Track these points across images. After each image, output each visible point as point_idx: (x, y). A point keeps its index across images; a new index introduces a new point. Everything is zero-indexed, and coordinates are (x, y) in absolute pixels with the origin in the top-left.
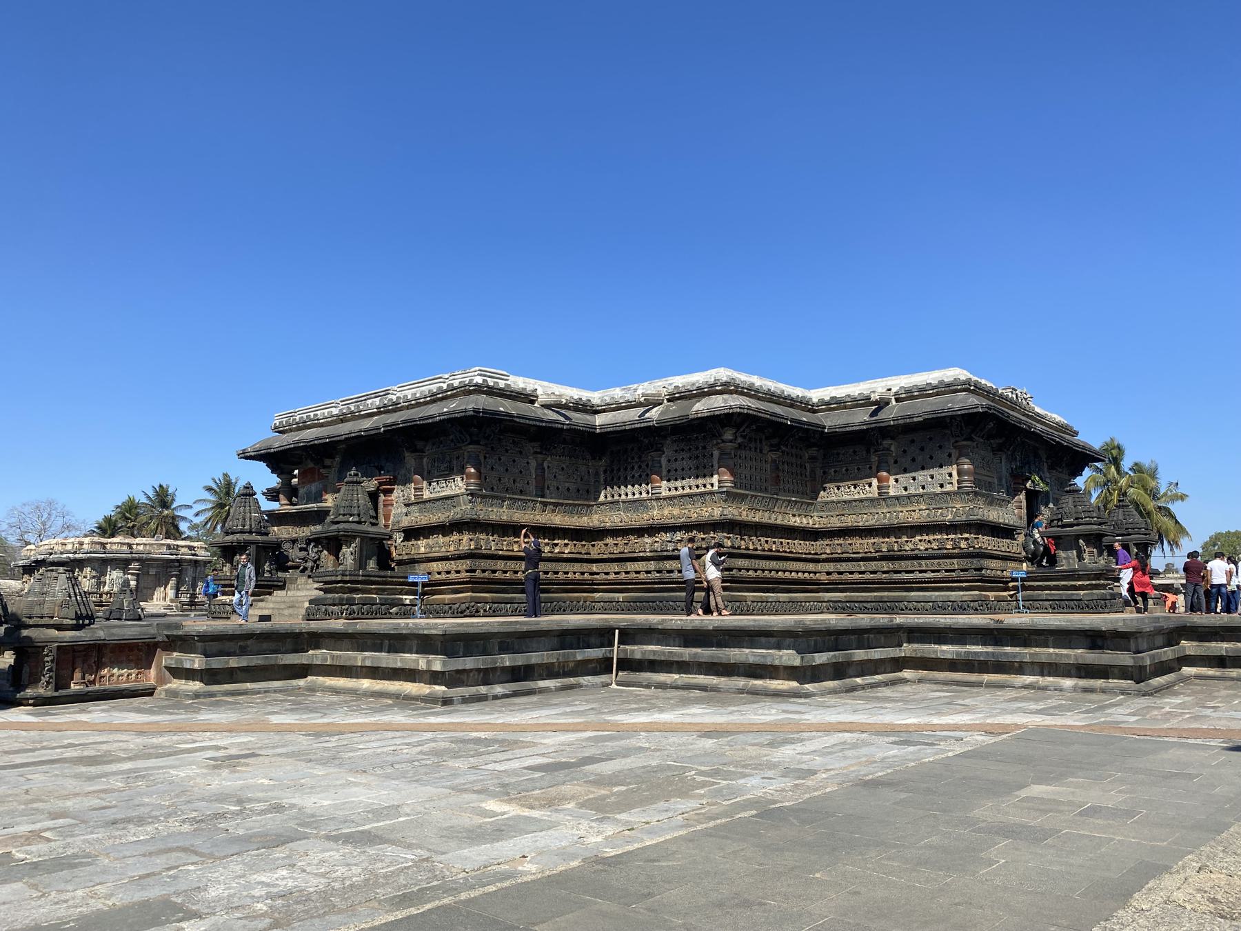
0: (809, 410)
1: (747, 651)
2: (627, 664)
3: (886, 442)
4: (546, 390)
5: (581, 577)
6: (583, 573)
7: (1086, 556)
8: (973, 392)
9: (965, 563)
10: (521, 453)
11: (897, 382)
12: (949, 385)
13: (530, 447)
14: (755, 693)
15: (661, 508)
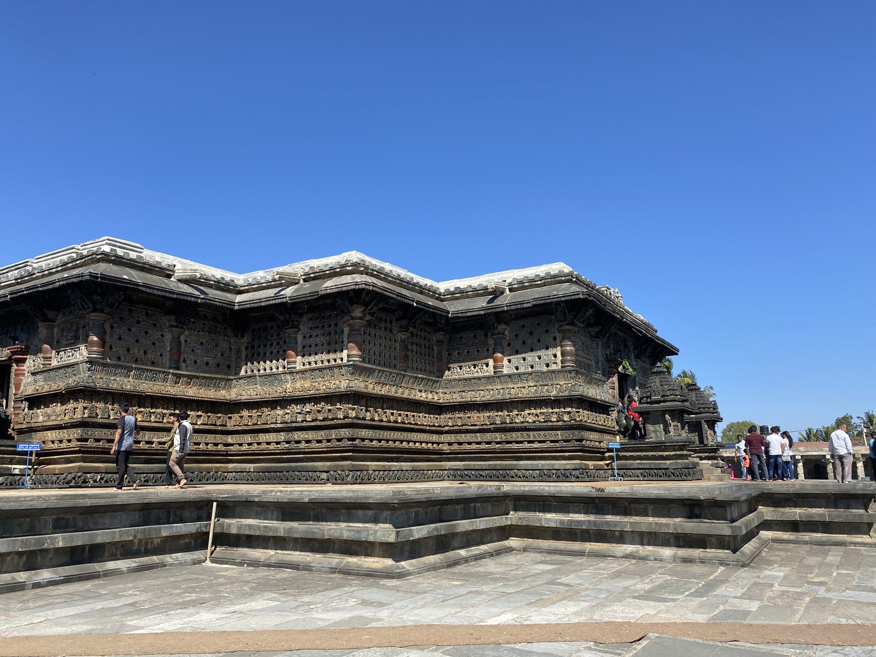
0: (437, 299)
1: (343, 525)
2: (223, 539)
3: (501, 327)
4: (183, 266)
5: (214, 448)
6: (216, 445)
7: (671, 429)
8: (576, 283)
9: (568, 434)
10: (155, 325)
11: (511, 274)
12: (555, 276)
13: (167, 320)
14: (347, 572)
15: (294, 381)
